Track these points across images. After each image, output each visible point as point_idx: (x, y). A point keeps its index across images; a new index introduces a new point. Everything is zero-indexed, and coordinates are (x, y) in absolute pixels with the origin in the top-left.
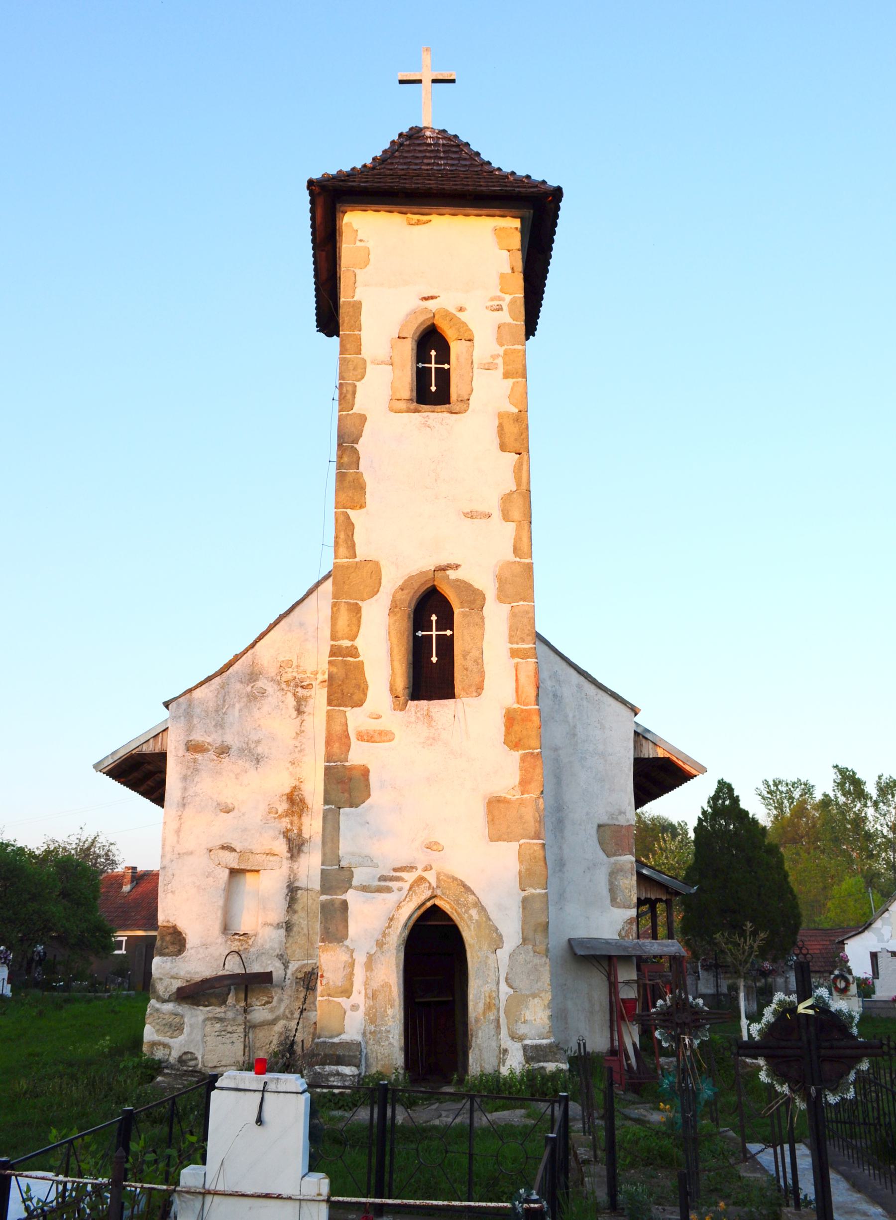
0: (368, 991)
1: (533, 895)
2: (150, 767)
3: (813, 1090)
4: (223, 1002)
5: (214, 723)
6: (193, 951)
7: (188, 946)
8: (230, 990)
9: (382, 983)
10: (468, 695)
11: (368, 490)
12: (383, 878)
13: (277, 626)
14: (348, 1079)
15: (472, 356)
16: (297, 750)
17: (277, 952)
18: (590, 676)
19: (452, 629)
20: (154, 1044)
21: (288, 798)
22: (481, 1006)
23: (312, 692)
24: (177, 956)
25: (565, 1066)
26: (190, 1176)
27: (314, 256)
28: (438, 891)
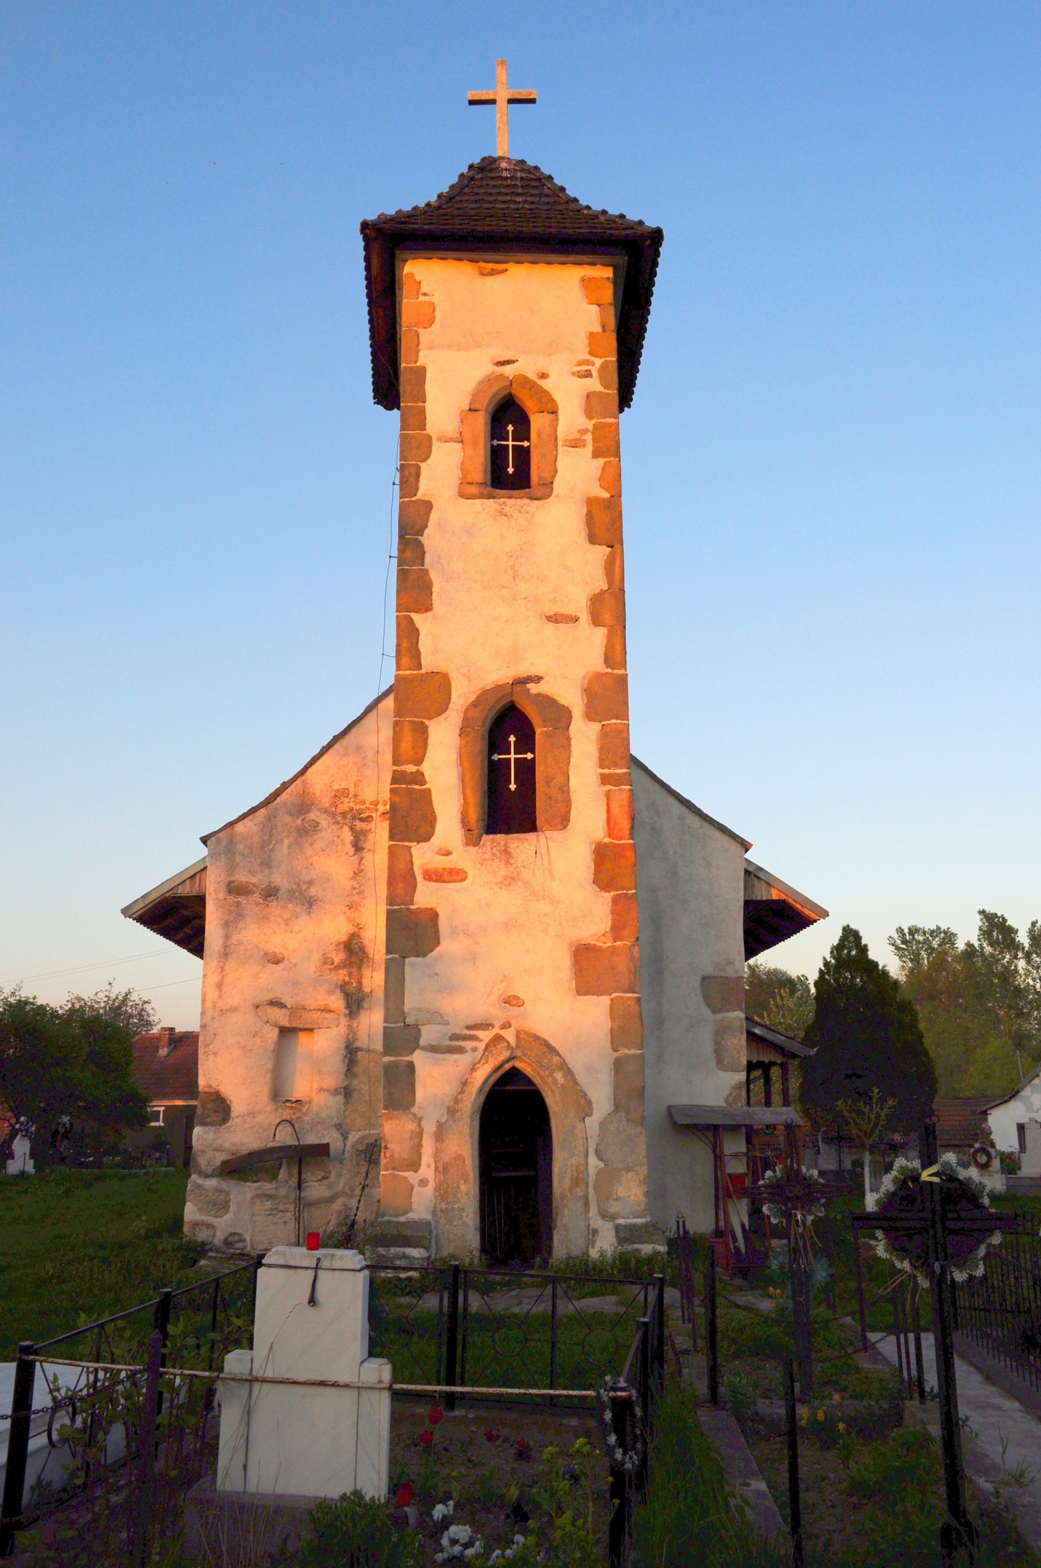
1: (626, 1056)
2: (186, 913)
3: (937, 1266)
4: (274, 1177)
5: (259, 861)
6: (238, 1120)
7: (233, 1114)
8: (281, 1164)
9: (454, 1155)
10: (552, 827)
11: (435, 589)
12: (454, 1037)
13: (331, 750)
15: (556, 431)
16: (355, 892)
17: (335, 1120)
18: (694, 806)
19: (533, 752)
20: (195, 1224)
21: (345, 947)
22: (567, 1182)
23: (373, 825)
24: (220, 1125)
25: (663, 1249)
26: (234, 1361)
27: (370, 313)
28: (518, 1052)
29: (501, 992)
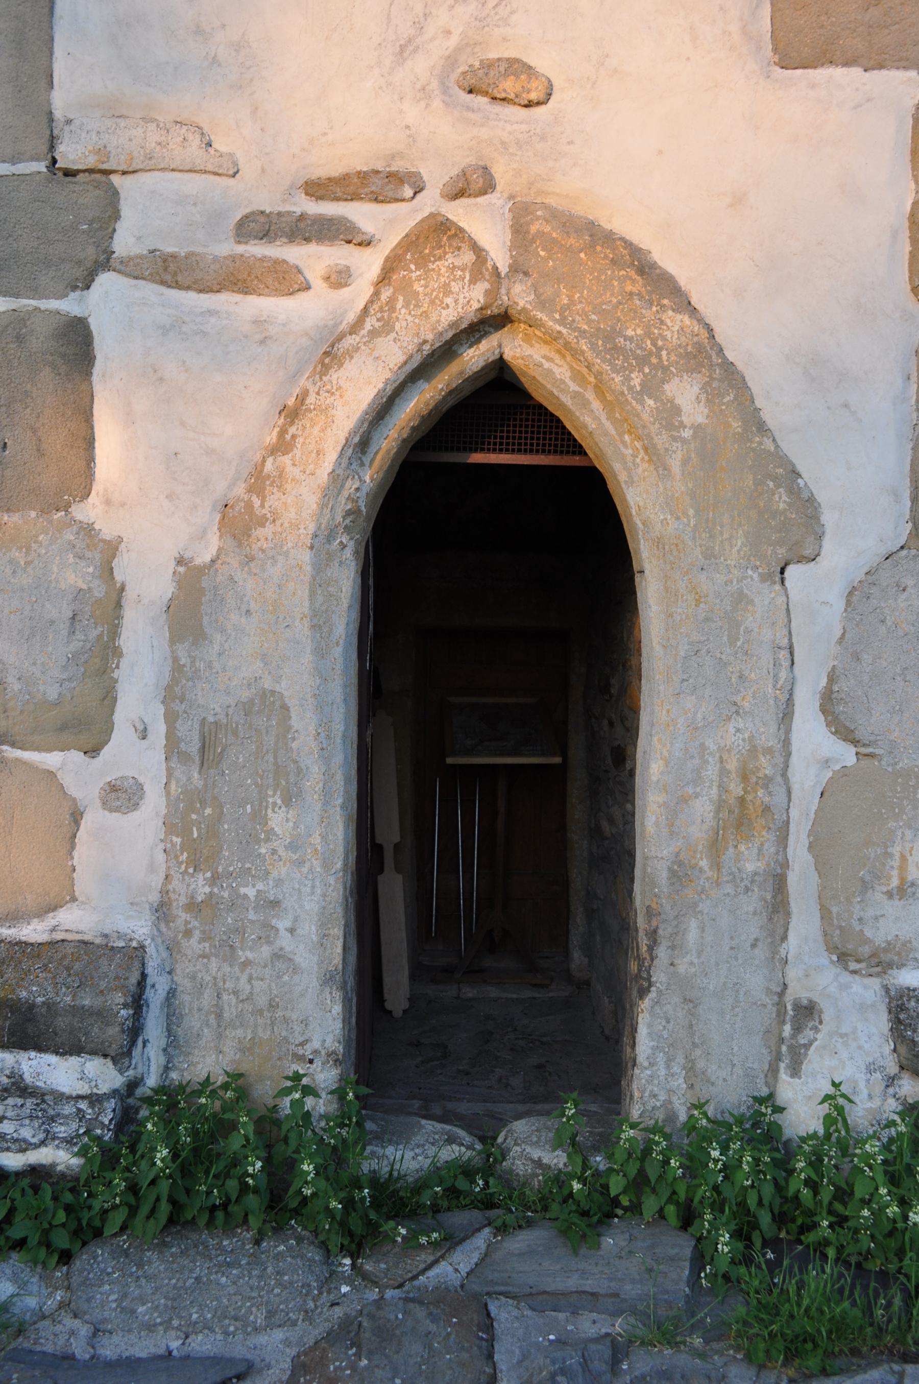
0: (182, 728)
9: (245, 695)
14: (68, 1109)
28: (518, 288)
29: (454, 40)
